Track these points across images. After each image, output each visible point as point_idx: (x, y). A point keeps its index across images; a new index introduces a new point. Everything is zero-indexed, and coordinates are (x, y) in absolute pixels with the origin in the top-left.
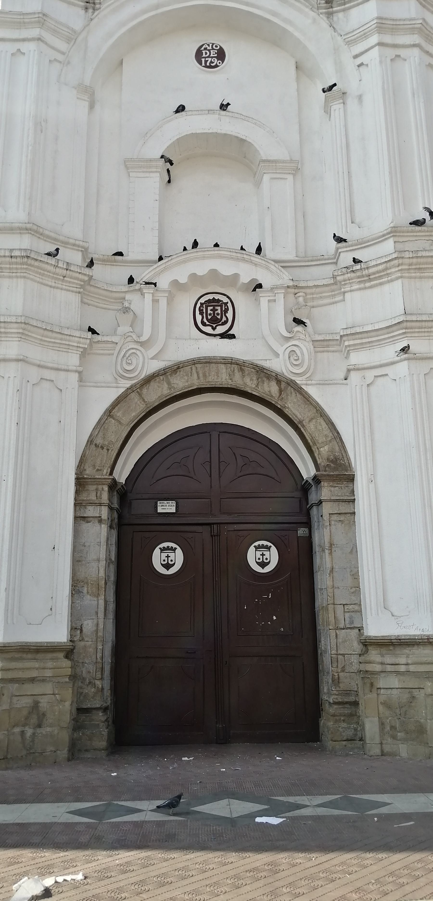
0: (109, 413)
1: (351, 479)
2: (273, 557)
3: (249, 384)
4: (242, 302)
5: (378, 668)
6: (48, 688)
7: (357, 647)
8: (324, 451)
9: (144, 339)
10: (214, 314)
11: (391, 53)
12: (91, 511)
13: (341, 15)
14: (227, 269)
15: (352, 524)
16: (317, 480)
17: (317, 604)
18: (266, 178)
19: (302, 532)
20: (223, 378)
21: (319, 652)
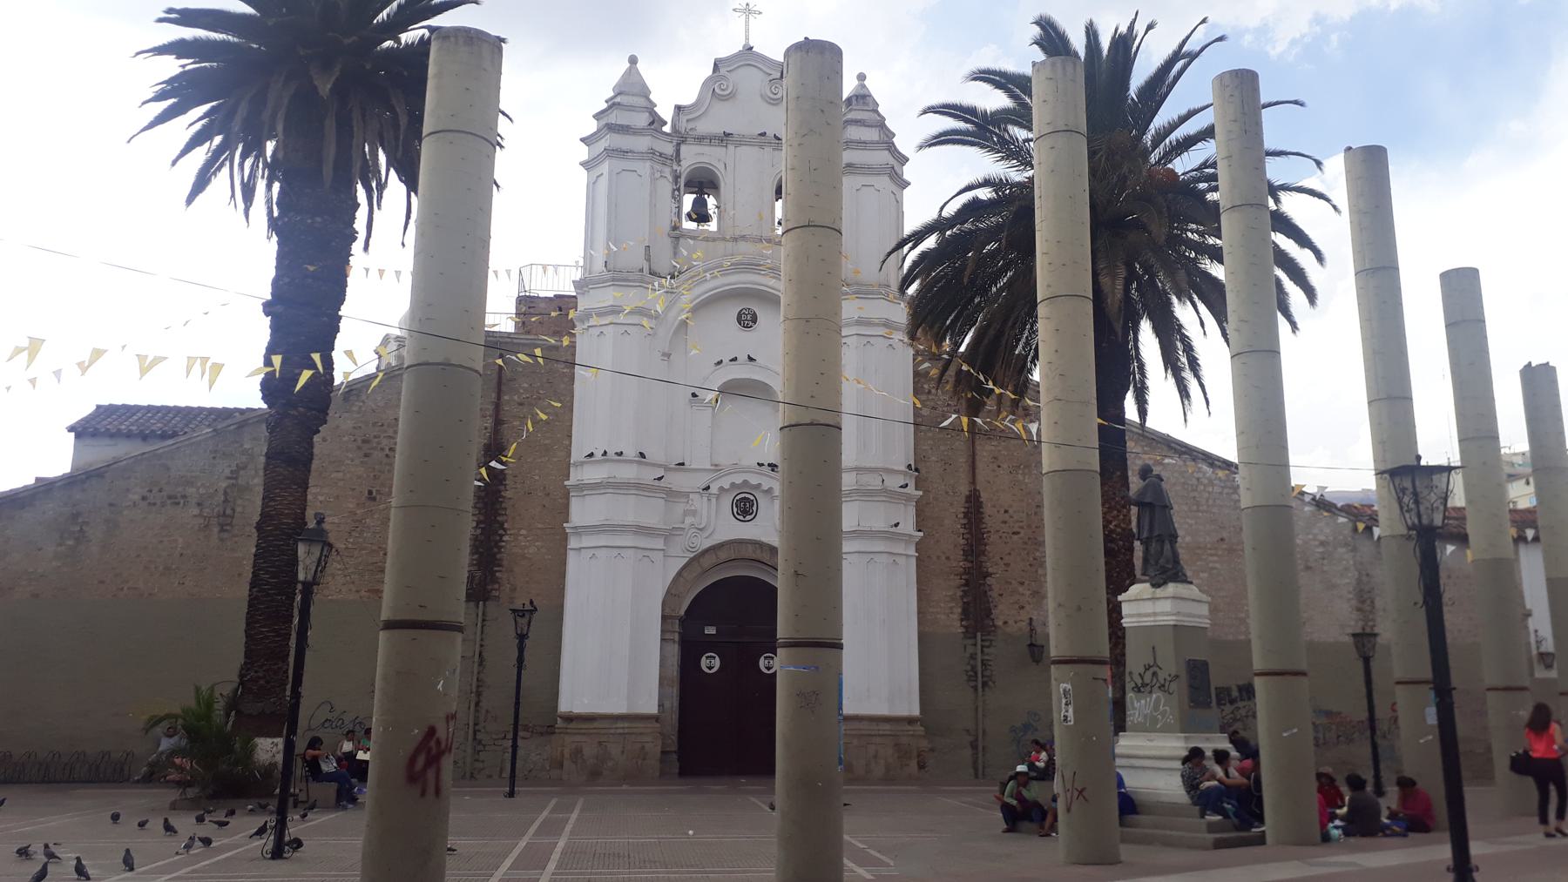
0: (679, 574)
4: (763, 502)
10: (745, 508)
11: (865, 340)
12: (668, 636)
14: (754, 480)
20: (749, 552)
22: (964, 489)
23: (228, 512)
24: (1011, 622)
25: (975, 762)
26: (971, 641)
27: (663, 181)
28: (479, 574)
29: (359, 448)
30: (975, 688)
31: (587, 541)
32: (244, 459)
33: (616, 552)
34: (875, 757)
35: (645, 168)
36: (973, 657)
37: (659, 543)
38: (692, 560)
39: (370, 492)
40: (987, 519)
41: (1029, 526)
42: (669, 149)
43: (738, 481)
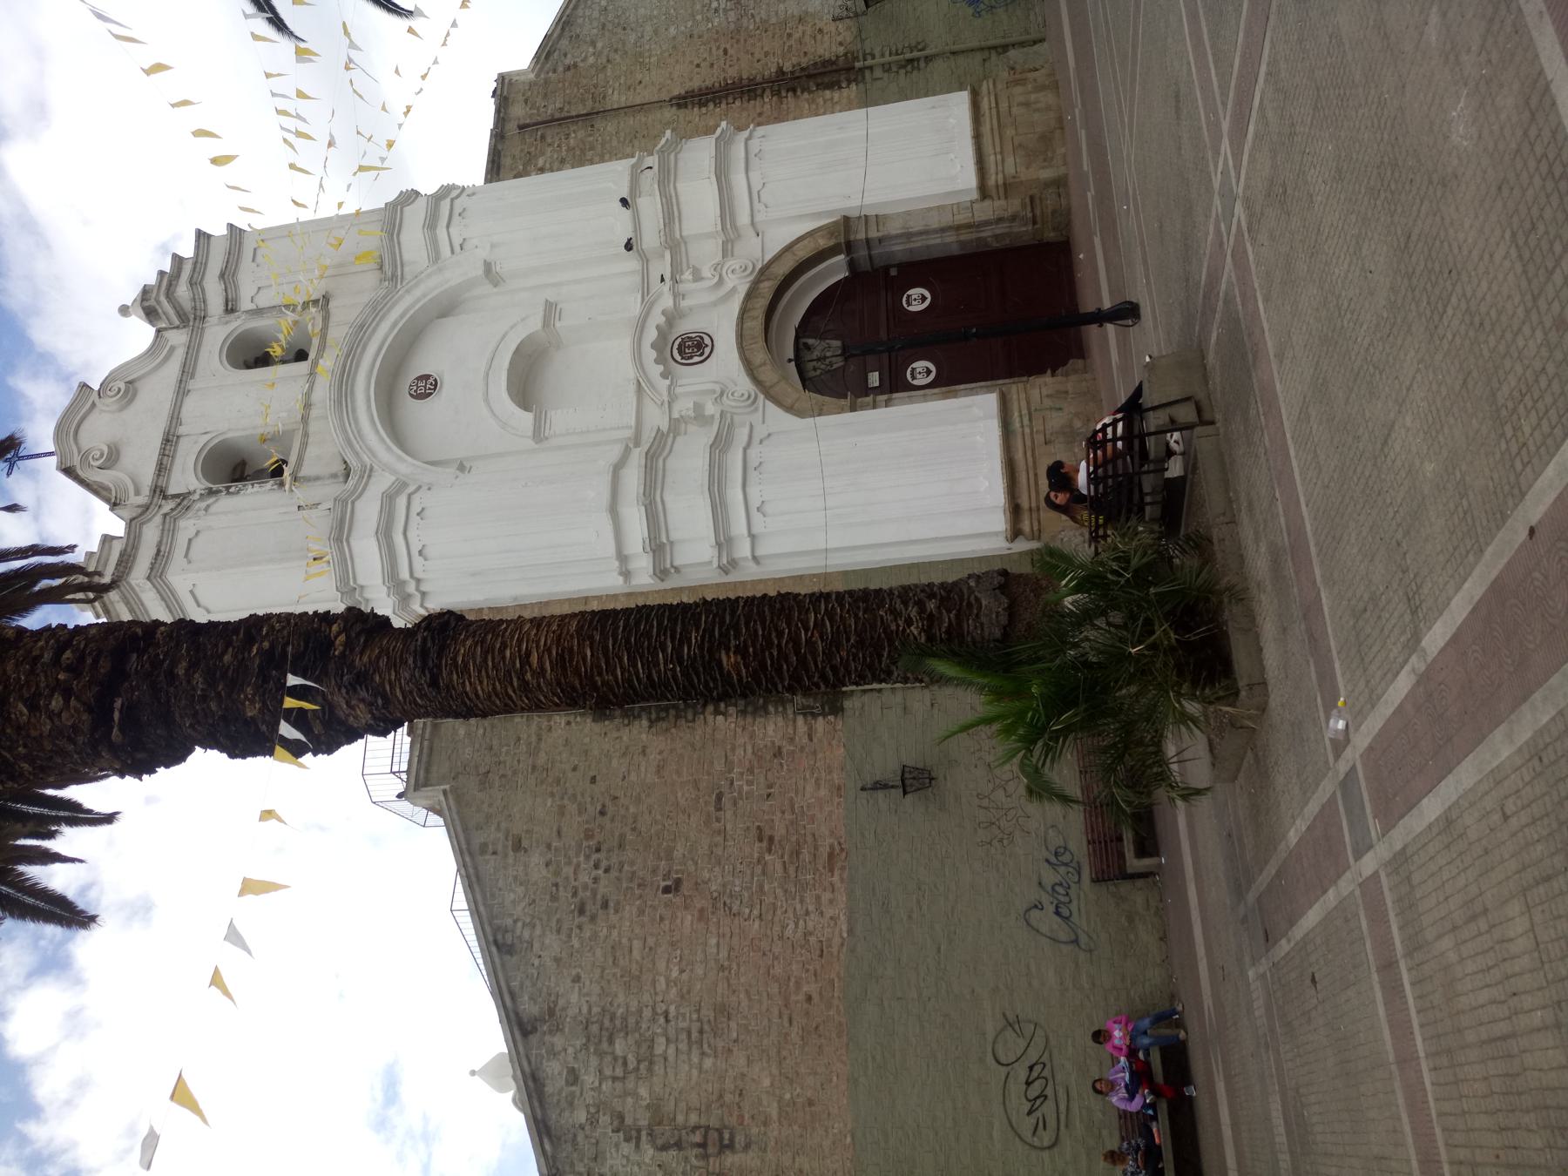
0: (789, 409)
1: (846, 219)
2: (916, 292)
3: (761, 304)
5: (1000, 176)
6: (1035, 394)
7: (987, 203)
8: (823, 243)
9: (718, 388)
10: (694, 348)
11: (456, 218)
13: (406, 269)
14: (651, 334)
15: (885, 217)
16: (849, 247)
17: (955, 250)
18: (558, 324)
19: (893, 272)
20: (756, 325)
21: (996, 245)
22: (669, 113)
23: (697, 1138)
24: (839, 39)
25: (1022, 44)
26: (867, 73)
27: (212, 509)
28: (799, 699)
29: (593, 918)
30: (928, 59)
31: (739, 527)
32: (604, 1119)
33: (752, 475)
34: (1027, 104)
35: (187, 526)
36: (887, 68)
37: (741, 435)
38: (769, 396)
39: (667, 890)
40: (708, 83)
41: (716, 40)
42: (168, 506)
43: (653, 354)
